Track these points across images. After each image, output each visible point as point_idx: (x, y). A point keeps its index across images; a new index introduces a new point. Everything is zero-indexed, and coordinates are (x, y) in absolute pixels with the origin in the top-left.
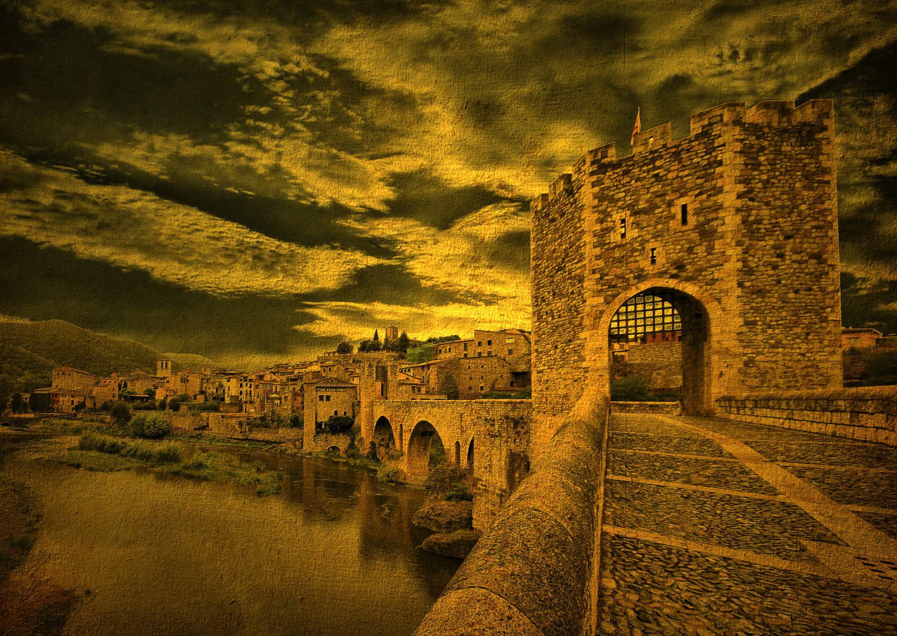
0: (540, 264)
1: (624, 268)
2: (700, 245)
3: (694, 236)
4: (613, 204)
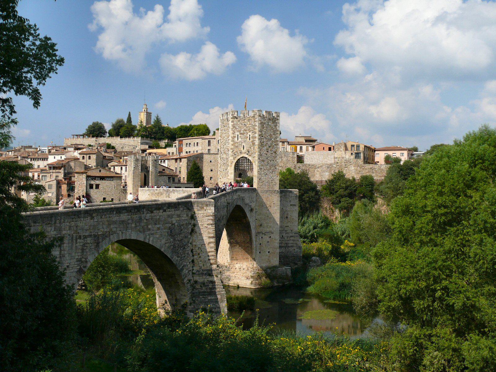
3: (251, 144)
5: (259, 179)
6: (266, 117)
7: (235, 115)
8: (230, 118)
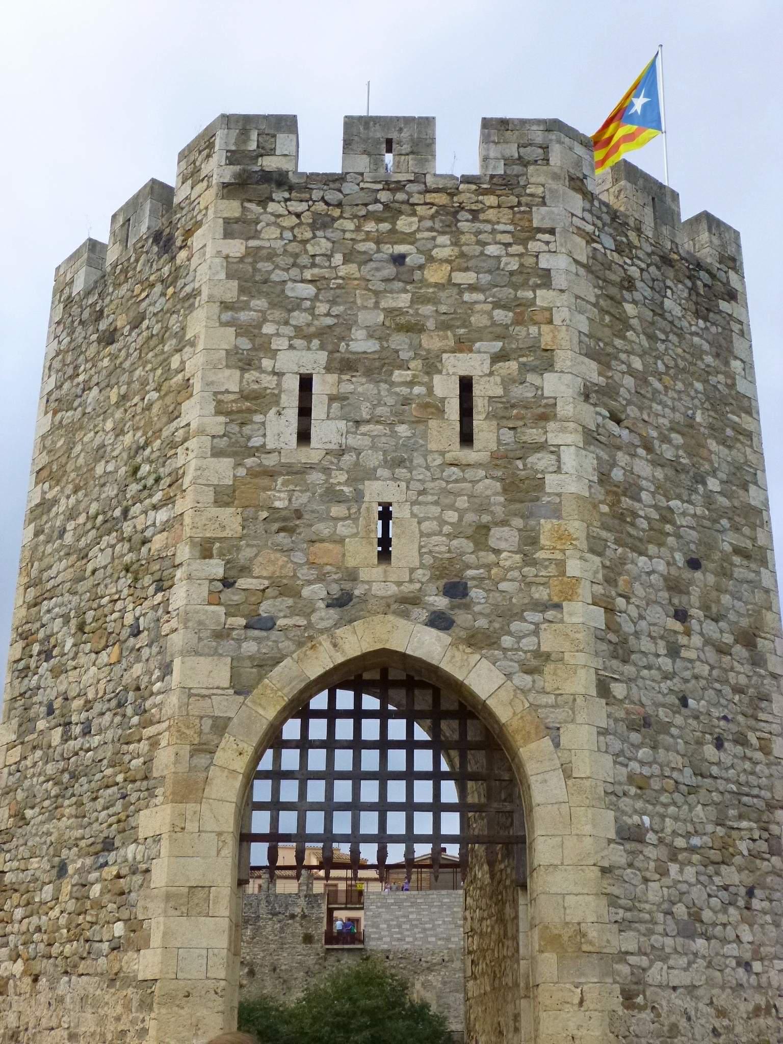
0: (55, 501)
1: (299, 557)
2: (504, 523)
3: (490, 488)
4: (278, 314)
5: (628, 997)
6: (639, 231)
7: (270, 163)
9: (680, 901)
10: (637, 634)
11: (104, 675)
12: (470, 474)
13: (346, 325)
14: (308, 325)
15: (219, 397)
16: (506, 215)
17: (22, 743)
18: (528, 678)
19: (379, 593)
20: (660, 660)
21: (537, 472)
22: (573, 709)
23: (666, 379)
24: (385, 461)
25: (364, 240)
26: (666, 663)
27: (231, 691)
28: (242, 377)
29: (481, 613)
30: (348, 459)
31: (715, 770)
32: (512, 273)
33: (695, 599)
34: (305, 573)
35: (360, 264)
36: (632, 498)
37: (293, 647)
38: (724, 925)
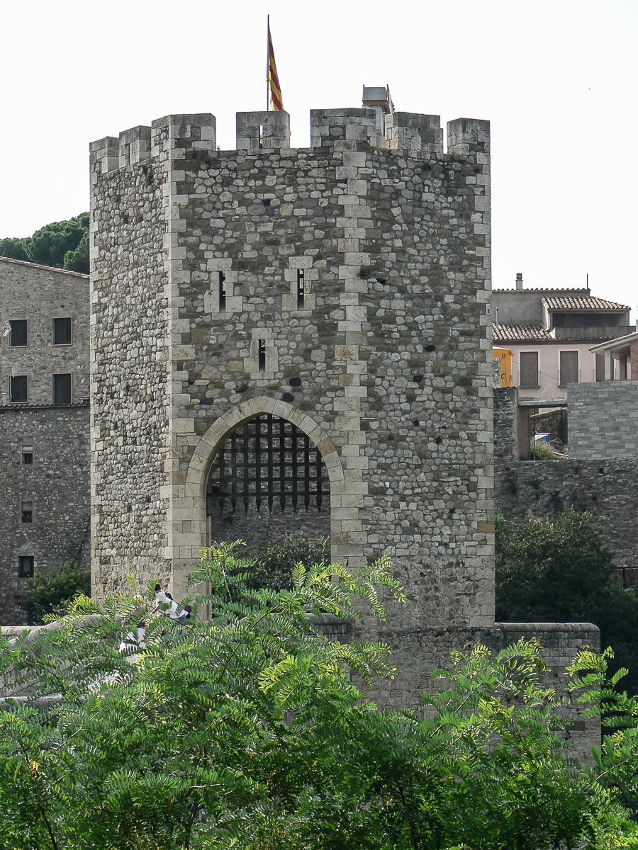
1: (222, 369)
2: (318, 347)
3: (312, 329)
4: (206, 238)
6: (406, 156)
7: (198, 145)
8: (168, 166)
9: (406, 519)
10: (388, 395)
11: (140, 416)
12: (302, 322)
13: (241, 242)
14: (222, 243)
15: (181, 286)
16: (321, 172)
17: (104, 440)
18: (328, 424)
19: (260, 386)
20: (401, 405)
21: (335, 320)
22: (348, 438)
23: (420, 246)
24: (262, 317)
25: (248, 192)
26: (406, 406)
27: (195, 434)
28: (191, 274)
29: (307, 394)
30: (244, 317)
31: (434, 455)
32: (324, 208)
33: (428, 369)
34: (226, 377)
35: (247, 206)
36: (389, 323)
37: (222, 412)
38: (433, 528)
